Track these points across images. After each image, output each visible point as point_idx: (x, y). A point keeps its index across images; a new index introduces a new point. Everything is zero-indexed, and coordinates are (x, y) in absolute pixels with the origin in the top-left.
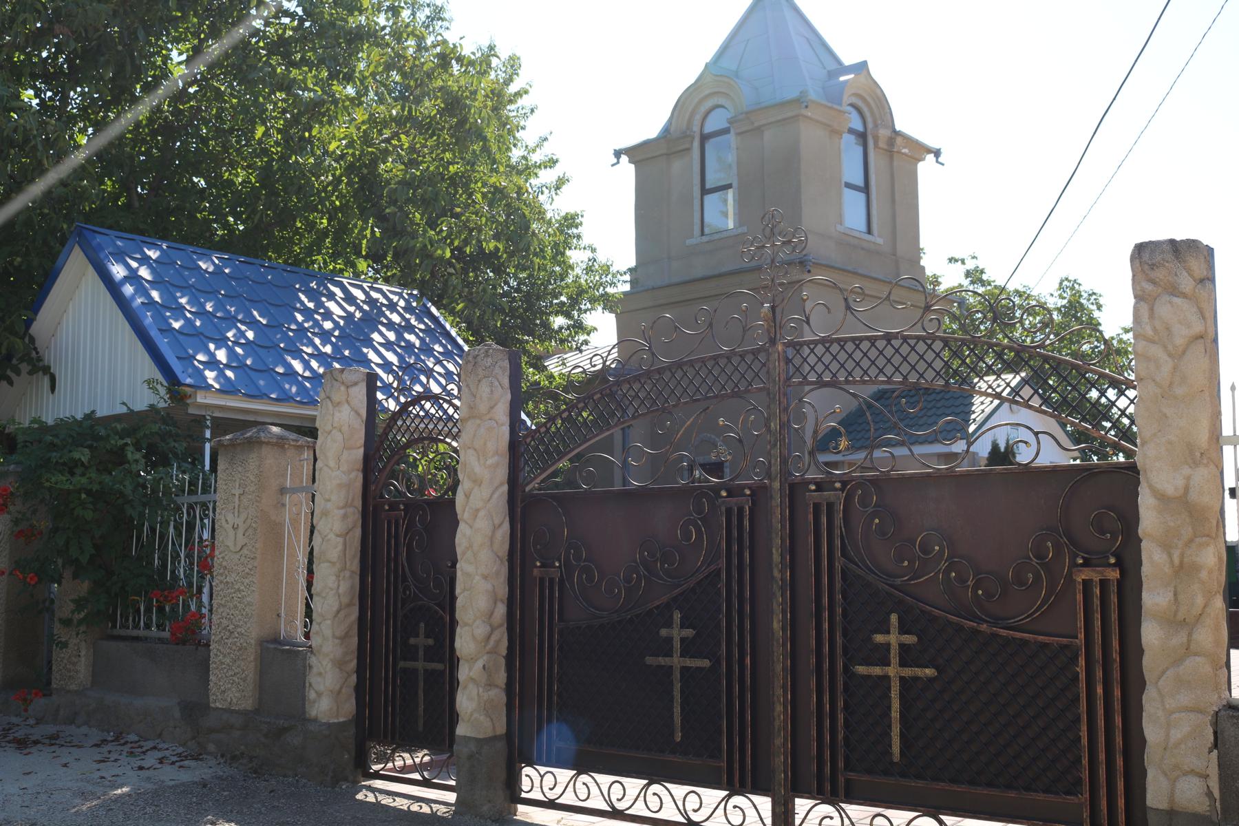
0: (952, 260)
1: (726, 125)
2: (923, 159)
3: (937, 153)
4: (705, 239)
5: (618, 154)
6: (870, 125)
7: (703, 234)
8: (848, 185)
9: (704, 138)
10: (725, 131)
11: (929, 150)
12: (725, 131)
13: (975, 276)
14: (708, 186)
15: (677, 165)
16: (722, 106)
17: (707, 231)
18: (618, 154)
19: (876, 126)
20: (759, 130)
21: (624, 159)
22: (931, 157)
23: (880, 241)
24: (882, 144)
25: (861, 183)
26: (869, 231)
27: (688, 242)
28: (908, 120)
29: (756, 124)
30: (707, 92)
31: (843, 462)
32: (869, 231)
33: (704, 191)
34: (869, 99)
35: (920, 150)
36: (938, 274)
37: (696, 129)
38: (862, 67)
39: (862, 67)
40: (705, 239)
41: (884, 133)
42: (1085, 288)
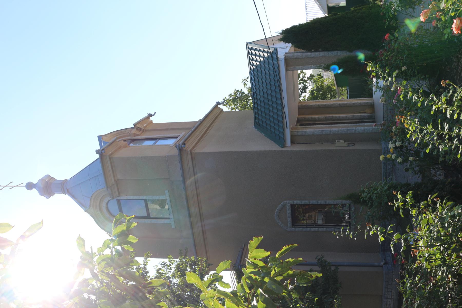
1: (115, 200)
2: (152, 121)
4: (172, 217)
6: (129, 138)
7: (169, 218)
10: (119, 201)
14: (145, 214)
16: (107, 204)
17: (167, 216)
19: (130, 135)
22: (151, 118)
23: (183, 133)
24: (139, 133)
27: (173, 226)
29: (114, 183)
31: (291, 132)
34: (117, 137)
38: (100, 138)
39: (100, 138)
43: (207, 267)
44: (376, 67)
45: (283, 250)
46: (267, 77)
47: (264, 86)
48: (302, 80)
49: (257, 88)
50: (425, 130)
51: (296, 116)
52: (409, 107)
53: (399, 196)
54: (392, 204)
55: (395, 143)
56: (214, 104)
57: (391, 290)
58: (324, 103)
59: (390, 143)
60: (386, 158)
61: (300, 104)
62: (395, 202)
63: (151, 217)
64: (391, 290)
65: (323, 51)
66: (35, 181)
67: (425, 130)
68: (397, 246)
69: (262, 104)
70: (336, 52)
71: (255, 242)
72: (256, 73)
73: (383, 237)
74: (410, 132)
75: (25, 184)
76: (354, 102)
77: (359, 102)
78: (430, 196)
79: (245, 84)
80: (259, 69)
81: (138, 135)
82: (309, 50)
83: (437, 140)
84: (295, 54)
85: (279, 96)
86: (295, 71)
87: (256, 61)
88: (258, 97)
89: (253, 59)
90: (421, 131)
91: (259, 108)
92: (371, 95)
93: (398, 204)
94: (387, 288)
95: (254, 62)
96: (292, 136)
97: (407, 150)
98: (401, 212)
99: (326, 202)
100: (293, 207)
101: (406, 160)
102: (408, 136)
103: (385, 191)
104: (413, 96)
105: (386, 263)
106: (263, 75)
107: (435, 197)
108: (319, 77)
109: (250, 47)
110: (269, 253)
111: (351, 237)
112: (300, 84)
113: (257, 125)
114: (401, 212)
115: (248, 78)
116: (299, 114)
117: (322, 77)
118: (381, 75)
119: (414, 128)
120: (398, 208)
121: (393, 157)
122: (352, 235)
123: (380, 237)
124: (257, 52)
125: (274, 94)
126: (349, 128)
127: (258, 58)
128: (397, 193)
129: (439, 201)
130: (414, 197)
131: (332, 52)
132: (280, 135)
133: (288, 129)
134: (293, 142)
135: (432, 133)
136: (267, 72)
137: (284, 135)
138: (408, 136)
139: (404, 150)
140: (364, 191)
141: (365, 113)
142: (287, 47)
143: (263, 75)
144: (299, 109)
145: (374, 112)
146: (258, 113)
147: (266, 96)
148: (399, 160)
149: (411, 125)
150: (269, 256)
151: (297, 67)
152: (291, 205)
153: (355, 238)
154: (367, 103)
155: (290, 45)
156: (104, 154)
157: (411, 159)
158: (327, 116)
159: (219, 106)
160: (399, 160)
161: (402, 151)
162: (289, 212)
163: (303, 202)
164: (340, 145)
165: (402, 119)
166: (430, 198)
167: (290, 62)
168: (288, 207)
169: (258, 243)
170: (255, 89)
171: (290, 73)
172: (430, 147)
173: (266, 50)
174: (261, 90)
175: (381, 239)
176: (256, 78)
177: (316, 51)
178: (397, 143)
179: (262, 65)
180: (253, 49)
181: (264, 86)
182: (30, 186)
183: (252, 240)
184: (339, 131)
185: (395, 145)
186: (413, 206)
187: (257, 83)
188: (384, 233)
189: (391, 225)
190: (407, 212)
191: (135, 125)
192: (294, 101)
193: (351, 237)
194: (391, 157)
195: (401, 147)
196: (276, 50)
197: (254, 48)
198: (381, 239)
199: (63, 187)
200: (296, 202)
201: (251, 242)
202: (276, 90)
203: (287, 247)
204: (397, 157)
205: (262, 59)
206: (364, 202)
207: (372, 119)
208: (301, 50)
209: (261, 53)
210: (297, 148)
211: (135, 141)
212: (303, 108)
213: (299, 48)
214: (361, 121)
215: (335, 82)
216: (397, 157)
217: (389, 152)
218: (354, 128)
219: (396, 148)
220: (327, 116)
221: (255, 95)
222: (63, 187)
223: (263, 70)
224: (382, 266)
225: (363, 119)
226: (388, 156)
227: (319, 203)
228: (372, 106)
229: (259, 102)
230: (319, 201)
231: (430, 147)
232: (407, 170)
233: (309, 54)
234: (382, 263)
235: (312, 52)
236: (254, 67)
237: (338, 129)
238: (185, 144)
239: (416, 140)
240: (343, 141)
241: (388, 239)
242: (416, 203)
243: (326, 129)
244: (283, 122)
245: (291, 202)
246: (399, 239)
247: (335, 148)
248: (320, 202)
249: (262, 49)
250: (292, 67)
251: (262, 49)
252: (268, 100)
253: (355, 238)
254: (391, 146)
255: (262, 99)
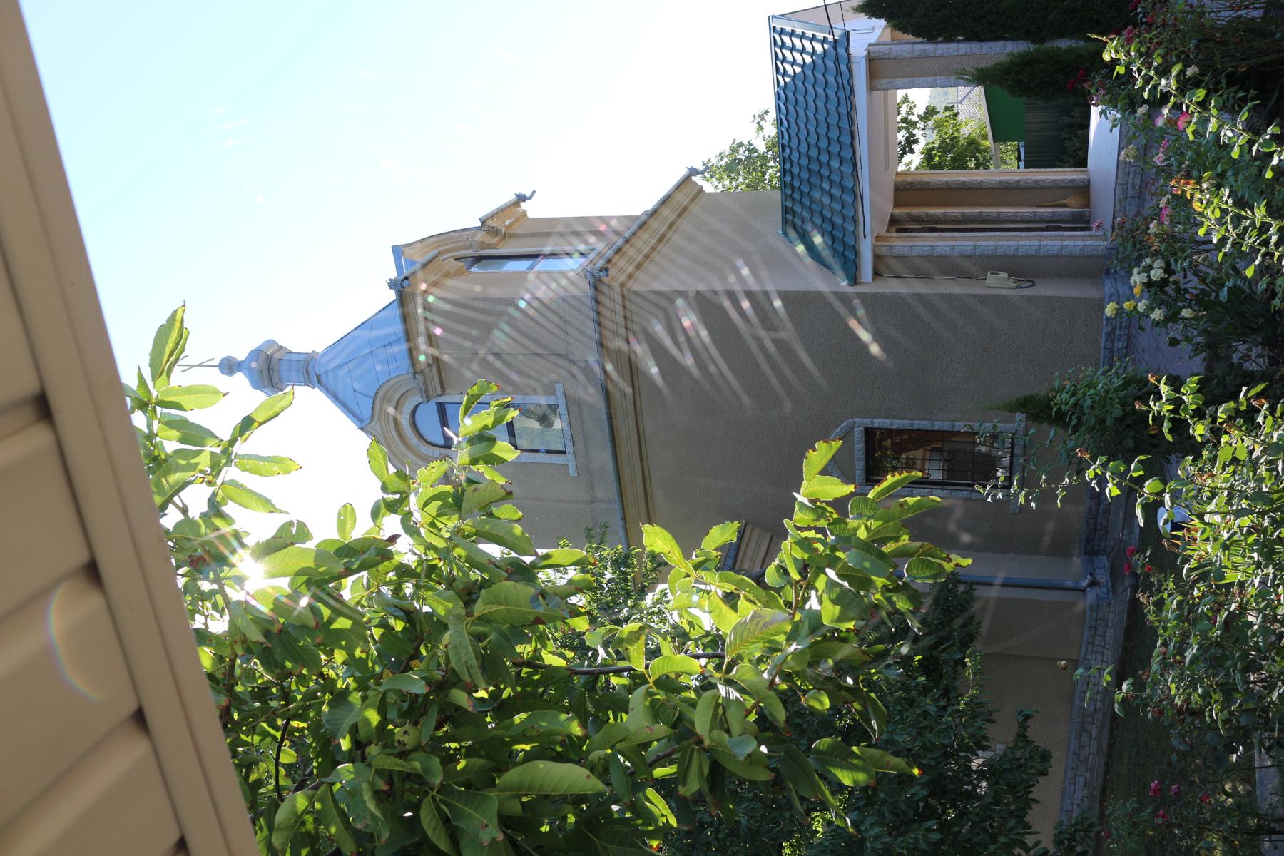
2: (524, 213)
4: (569, 449)
6: (469, 252)
7: (564, 452)
19: (471, 247)
24: (494, 240)
27: (573, 473)
30: (394, 433)
38: (398, 251)
39: (398, 251)
40: (569, 449)
43: (654, 569)
44: (1128, 53)
45: (885, 485)
46: (821, 105)
47: (812, 129)
48: (905, 120)
49: (793, 134)
50: (1246, 218)
51: (888, 208)
52: (1208, 160)
53: (1165, 390)
54: (1145, 408)
55: (1148, 272)
56: (682, 173)
57: (1100, 649)
58: (962, 179)
59: (1135, 271)
60: (1120, 311)
61: (899, 179)
62: (1152, 403)
64: (1100, 649)
65: (968, 39)
66: (241, 356)
67: (1246, 218)
68: (1152, 509)
69: (805, 175)
70: (1000, 43)
71: (820, 454)
72: (790, 95)
73: (1118, 485)
74: (1206, 223)
75: (216, 362)
76: (1038, 178)
77: (1052, 177)
78: (1244, 389)
79: (760, 128)
80: (799, 84)
81: (489, 246)
82: (931, 38)
83: (1277, 245)
84: (895, 48)
85: (847, 154)
86: (890, 92)
87: (794, 63)
88: (795, 156)
89: (784, 60)
90: (1237, 220)
91: (796, 183)
92: (1083, 163)
93: (1161, 406)
94: (1093, 643)
95: (788, 67)
96: (877, 257)
97: (1178, 290)
98: (1166, 426)
99: (953, 426)
100: (869, 433)
101: (1172, 317)
102: (1201, 232)
103: (1117, 390)
104: (1221, 127)
105: (1093, 584)
106: (810, 101)
107: (1257, 396)
108: (948, 113)
109: (778, 28)
110: (851, 488)
111: (1022, 500)
112: (900, 129)
114: (1166, 426)
115: (767, 112)
116: (896, 205)
117: (956, 115)
118: (1140, 71)
119: (1218, 213)
120: (1159, 419)
121: (1142, 307)
122: (1026, 496)
123: (1110, 485)
124: (797, 41)
125: (835, 148)
126: (1022, 243)
127: (797, 56)
128: (1159, 381)
129: (1266, 406)
130: (1202, 388)
131: (992, 44)
132: (846, 253)
133: (868, 237)
134: (877, 274)
135: (1265, 228)
136: (820, 91)
137: (856, 253)
138: (1201, 232)
139: (1170, 290)
140: (1061, 390)
141: (1065, 206)
142: (873, 29)
143: (810, 101)
144: (896, 190)
145: (1088, 205)
146: (791, 196)
147: (814, 153)
148: (1157, 315)
149: (1210, 209)
150: (852, 495)
151: (898, 81)
152: (866, 430)
153: (1033, 505)
154: (1072, 181)
155: (880, 23)
156: (408, 290)
157: (1186, 313)
158: (968, 210)
159: (694, 179)
160: (1157, 315)
161: (1165, 293)
162: (859, 446)
163: (897, 424)
164: (998, 283)
165: (1188, 188)
166: (1245, 395)
167: (881, 69)
168: (858, 436)
169: (830, 456)
170: (786, 136)
171: (878, 95)
172: (1257, 262)
173: (820, 36)
174: (803, 138)
175: (1112, 490)
176: (791, 108)
177: (950, 39)
178: (1152, 273)
179: (809, 73)
180: (786, 34)
181: (812, 129)
183: (814, 450)
184: (996, 248)
185: (1149, 276)
186: (1199, 414)
187: (792, 121)
188: (1122, 476)
189: (1142, 458)
190: (1180, 426)
191: (483, 221)
192: (886, 167)
193: (1022, 500)
194: (1135, 307)
195: (1164, 283)
196: (847, 34)
197: (789, 29)
198: (1112, 490)
200: (878, 423)
201: (810, 454)
202: (842, 139)
203: (897, 477)
204: (1151, 308)
205: (808, 59)
206: (1060, 419)
207: (1081, 222)
208: (910, 37)
209: (807, 44)
210: (892, 287)
211: (484, 262)
212: (906, 191)
213: (904, 30)
214: (1053, 225)
215: (988, 128)
216: (1151, 308)
217: (1131, 297)
218: (1037, 243)
219: (1149, 284)
220: (968, 210)
221: (788, 150)
222: (309, 370)
223: (810, 87)
224: (1084, 591)
225: (1058, 222)
226: (1128, 305)
227: (936, 428)
228: (1084, 190)
229: (796, 170)
230: (937, 423)
231: (1257, 262)
232: (1174, 342)
233: (930, 47)
234: (1084, 584)
235: (937, 43)
236: (787, 80)
237: (993, 243)
238: (607, 270)
239: (1223, 240)
240: (1006, 275)
241: (1131, 489)
242: (1207, 404)
243: (963, 243)
244: (855, 220)
245: (867, 422)
246: (1161, 494)
247: (984, 292)
248: (938, 425)
249: (809, 34)
250: (884, 81)
251: (809, 34)
252: (820, 163)
253: (1033, 505)
254: (1137, 278)
255: (804, 162)
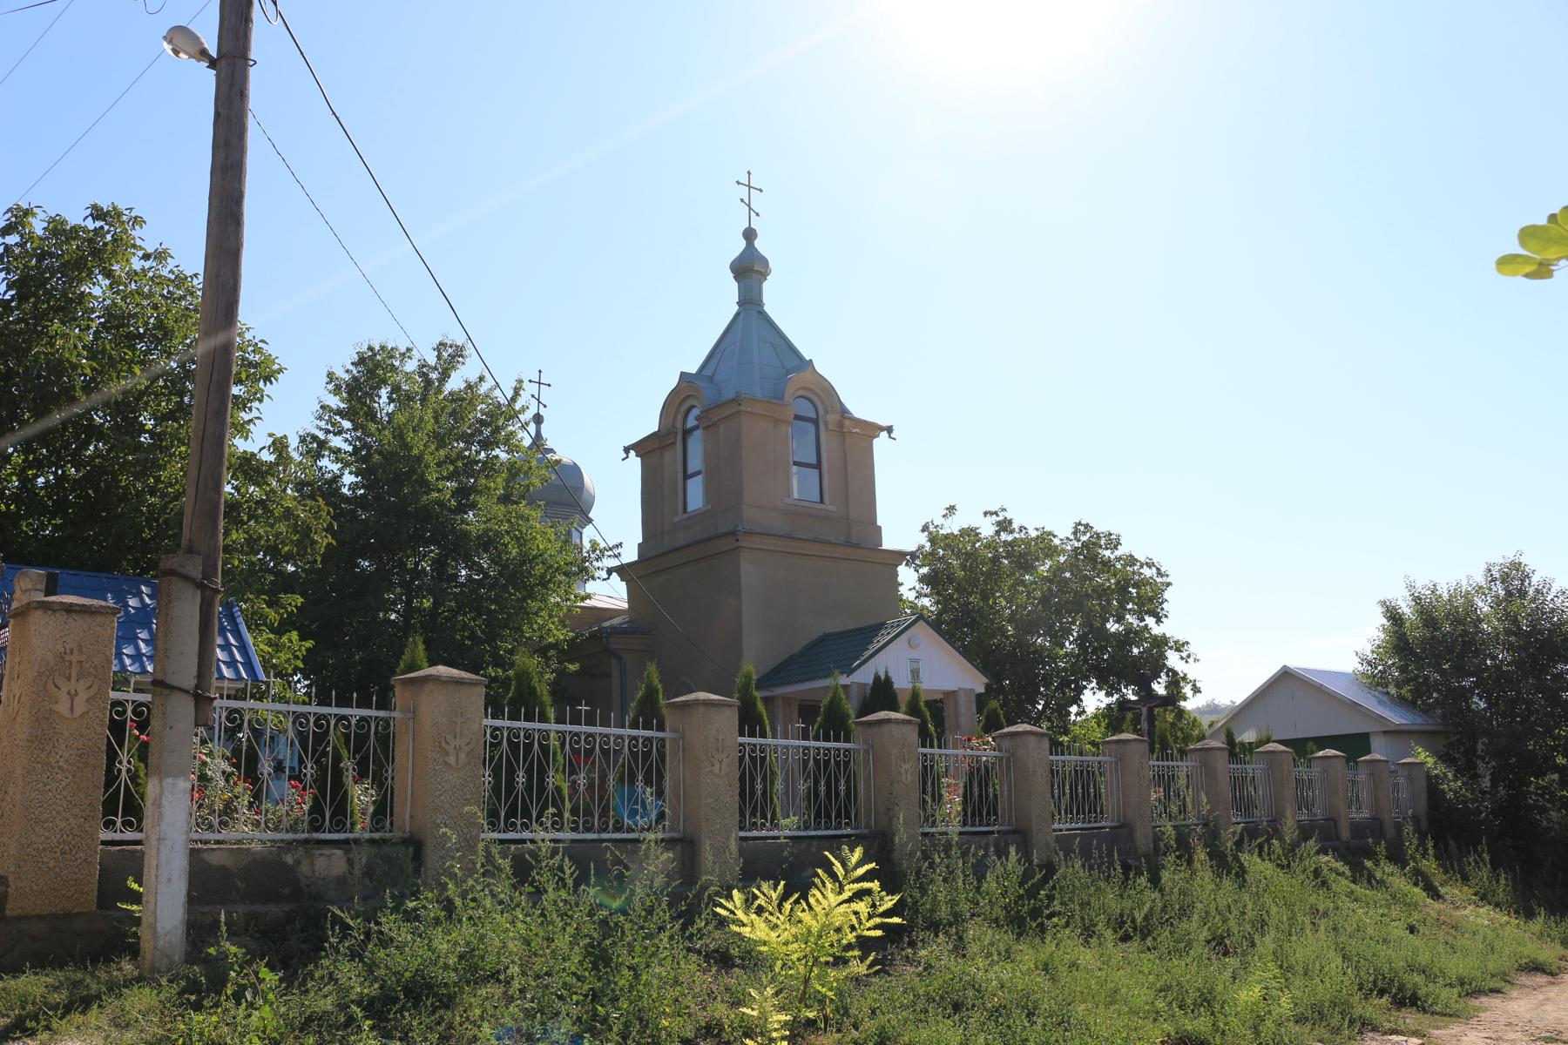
0: (986, 514)
3: (889, 430)
5: (627, 450)
6: (821, 411)
8: (795, 463)
9: (687, 433)
10: (695, 428)
11: (882, 429)
12: (695, 428)
13: (1005, 526)
14: (690, 470)
15: (668, 456)
17: (690, 508)
18: (627, 450)
20: (715, 425)
21: (632, 453)
22: (884, 434)
25: (813, 461)
26: (822, 501)
27: (677, 519)
28: (859, 405)
32: (822, 501)
33: (686, 477)
35: (872, 430)
36: (974, 525)
37: (679, 425)
41: (832, 418)
42: (1100, 527)
63: (690, 482)
66: (757, 244)
113: (825, 638)
182: (750, 235)
199: (750, 301)
222: (750, 301)
